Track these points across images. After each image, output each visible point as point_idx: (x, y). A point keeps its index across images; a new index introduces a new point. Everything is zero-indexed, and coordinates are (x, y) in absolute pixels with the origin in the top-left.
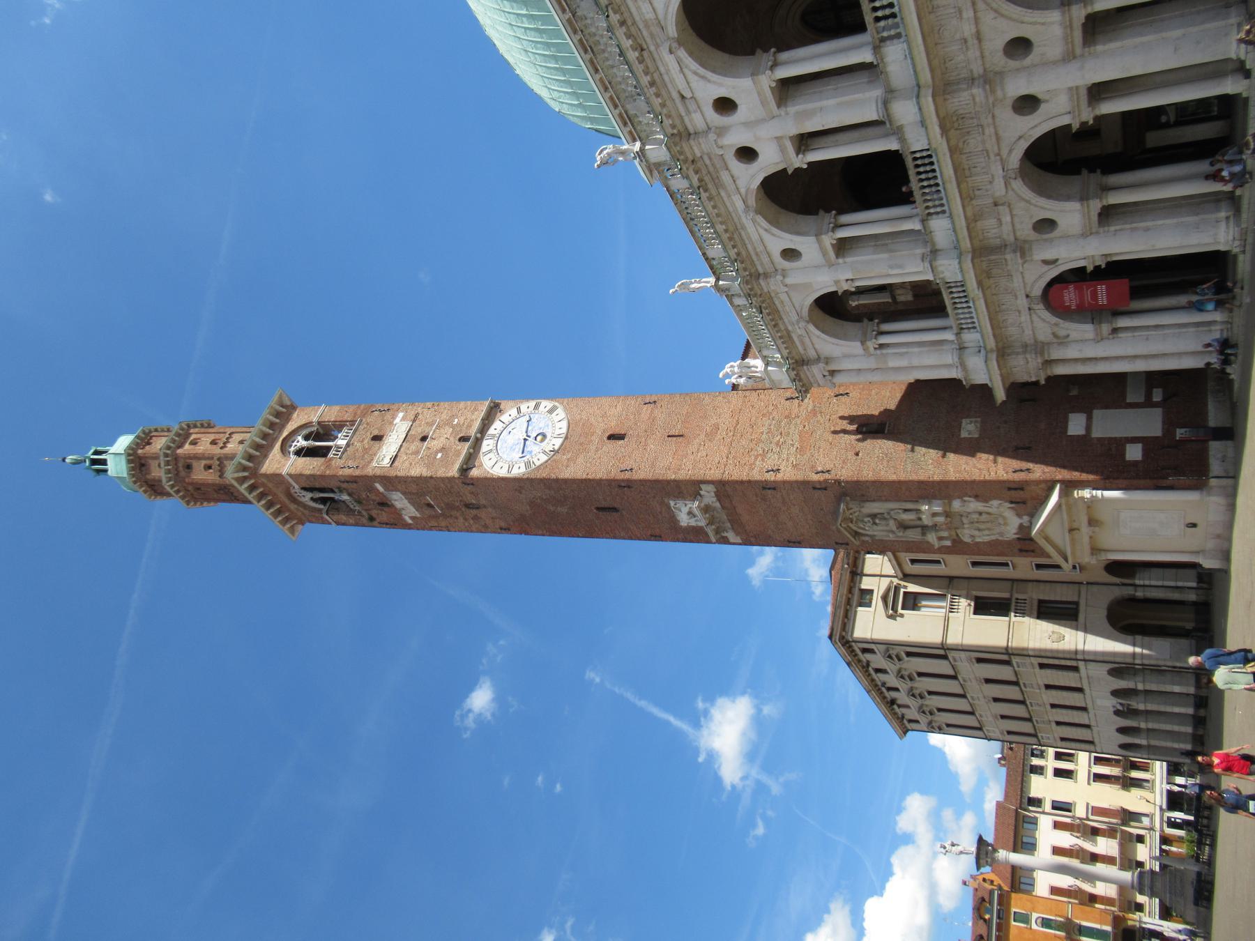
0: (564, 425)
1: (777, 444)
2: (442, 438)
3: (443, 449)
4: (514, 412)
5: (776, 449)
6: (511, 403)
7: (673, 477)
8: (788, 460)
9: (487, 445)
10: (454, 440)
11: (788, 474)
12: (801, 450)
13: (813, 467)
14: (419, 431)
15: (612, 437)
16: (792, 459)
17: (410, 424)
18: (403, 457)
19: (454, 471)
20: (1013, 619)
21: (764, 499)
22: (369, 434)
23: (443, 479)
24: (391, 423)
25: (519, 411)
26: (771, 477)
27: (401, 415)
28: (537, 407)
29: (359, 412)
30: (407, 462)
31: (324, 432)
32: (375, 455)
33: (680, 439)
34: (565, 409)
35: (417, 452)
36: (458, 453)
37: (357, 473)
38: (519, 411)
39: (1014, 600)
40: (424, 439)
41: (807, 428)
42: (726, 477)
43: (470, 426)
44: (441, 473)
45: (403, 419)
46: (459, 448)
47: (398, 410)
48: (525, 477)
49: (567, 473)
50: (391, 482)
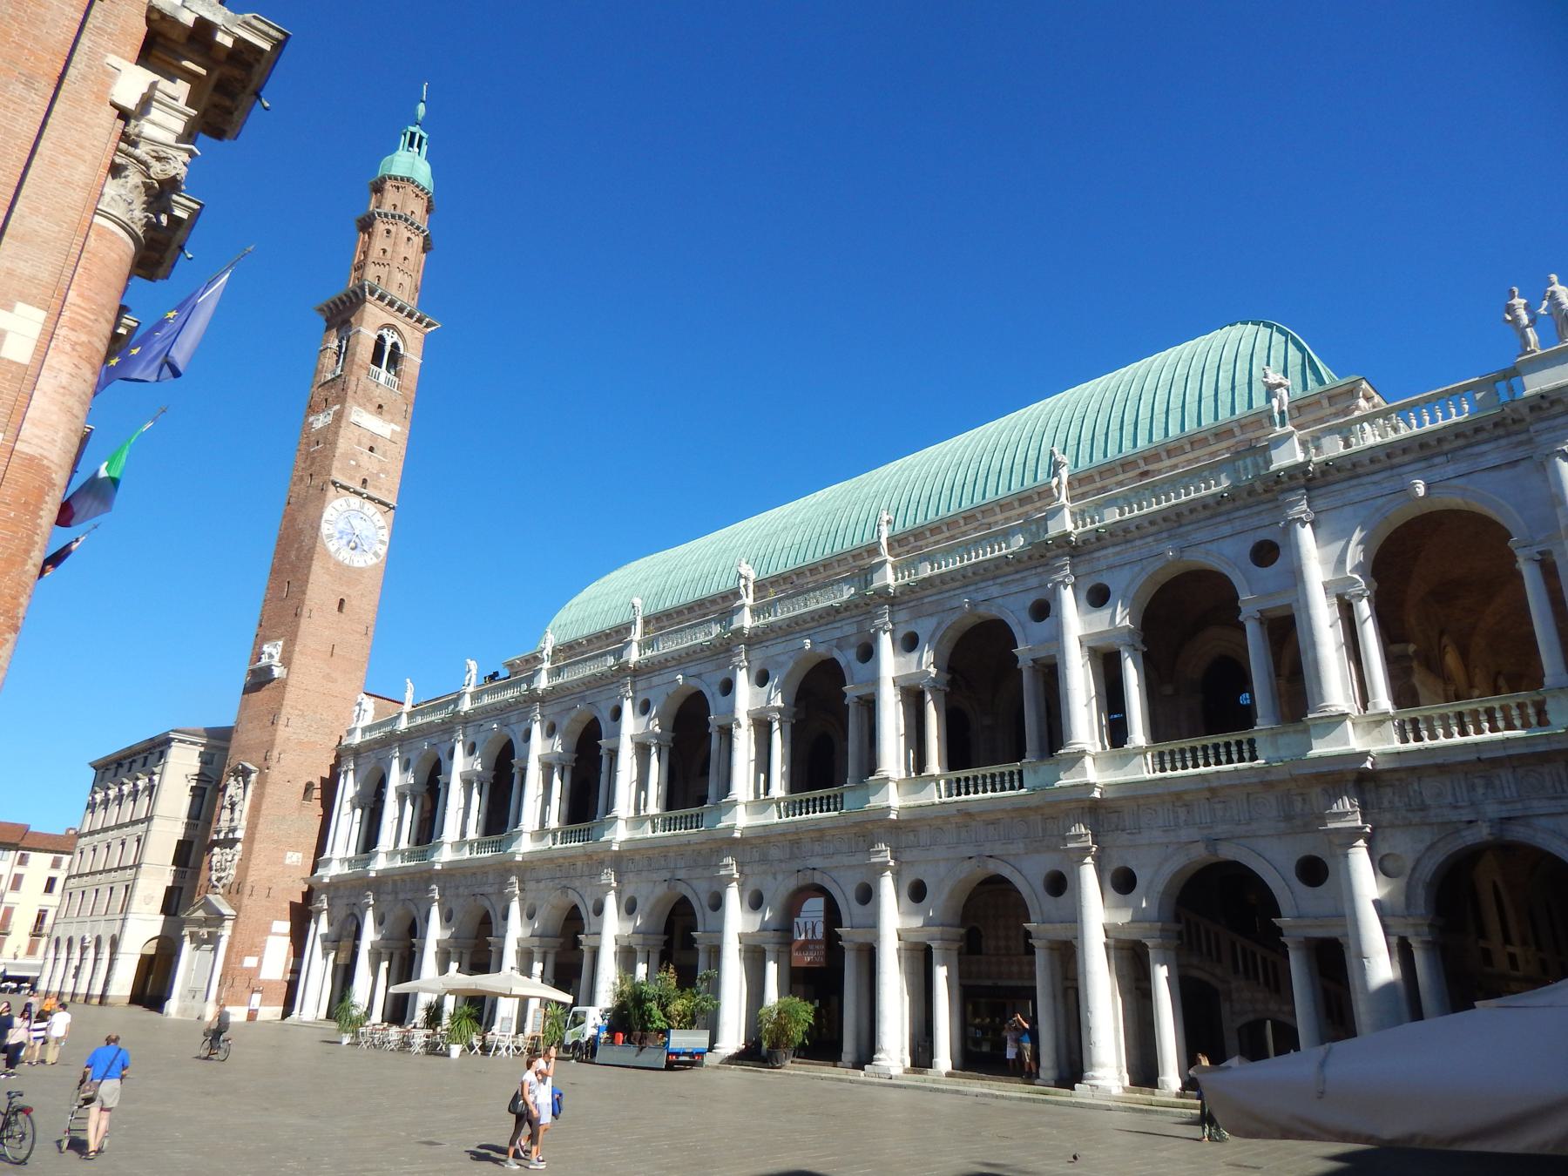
0: (362, 565)
1: (310, 726)
2: (369, 463)
3: (358, 466)
4: (382, 523)
5: (305, 725)
6: (391, 521)
7: (297, 649)
8: (294, 733)
9: (355, 501)
10: (364, 474)
11: (282, 732)
12: (300, 743)
13: (284, 751)
14: (379, 446)
15: (342, 601)
16: (295, 736)
17: (388, 438)
18: (357, 432)
19: (337, 476)
20: (169, 869)
21: (269, 713)
22: (386, 401)
23: (330, 465)
24: (392, 421)
25: (381, 528)
26: (282, 721)
27: (398, 429)
28: (382, 542)
29: (408, 392)
30: (351, 436)
31: (395, 358)
32: (365, 408)
33: (329, 654)
34: (376, 564)
35: (359, 444)
36: (352, 478)
37: (350, 393)
38: (381, 528)
39: (185, 869)
40: (371, 449)
41: (319, 746)
42: (289, 688)
43: (375, 487)
44: (336, 464)
45: (393, 431)
46: (357, 479)
47: (403, 426)
48: (319, 534)
49: (316, 567)
50: (339, 417)
